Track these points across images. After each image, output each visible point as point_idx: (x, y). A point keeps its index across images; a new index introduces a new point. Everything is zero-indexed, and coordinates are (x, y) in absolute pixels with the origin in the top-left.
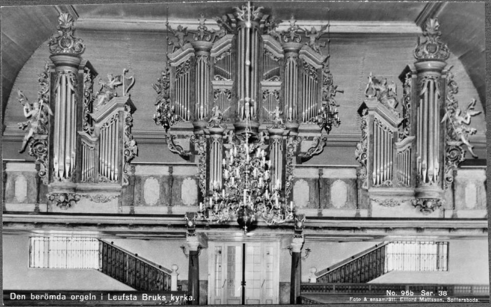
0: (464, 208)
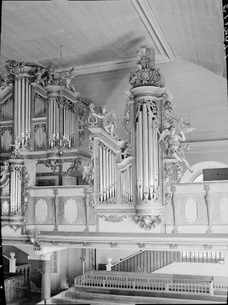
0: (186, 224)
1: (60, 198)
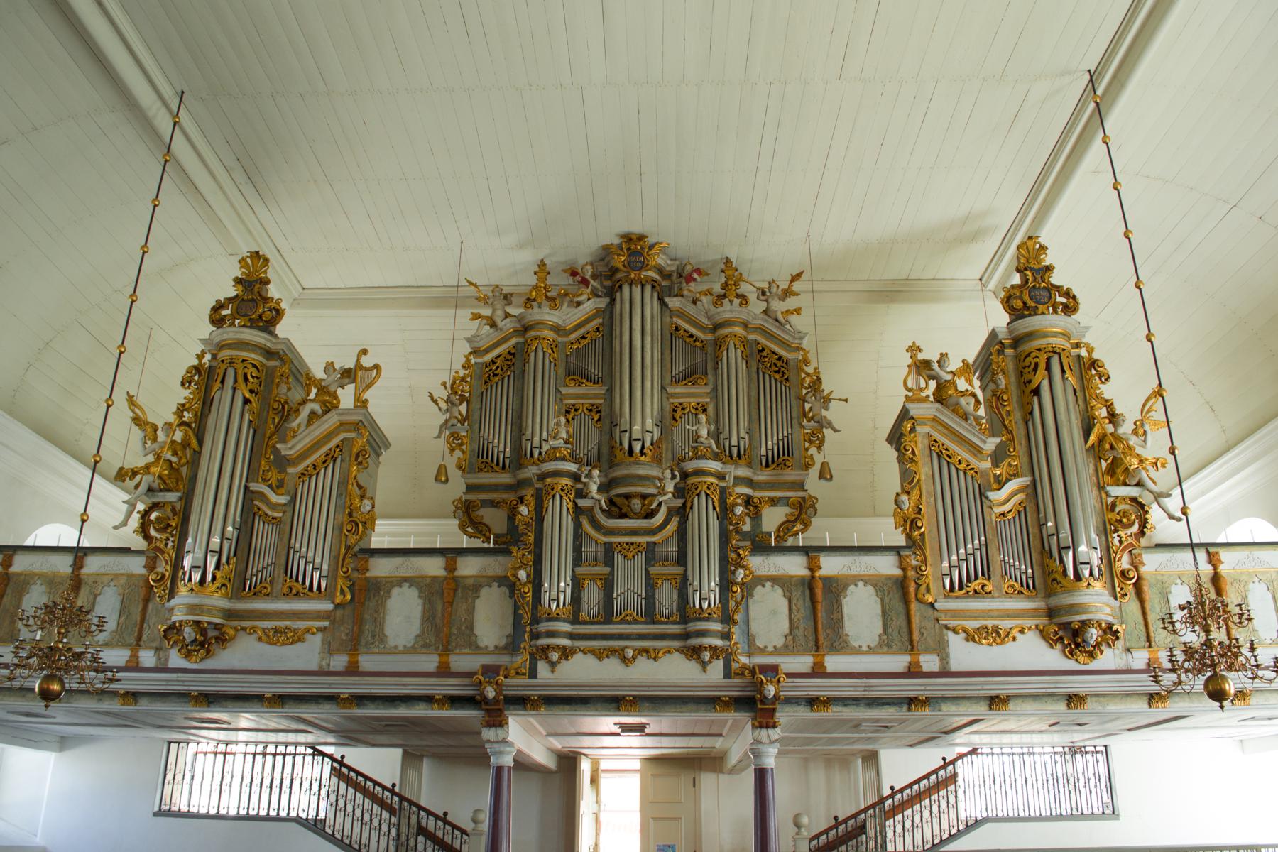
1: (828, 580)
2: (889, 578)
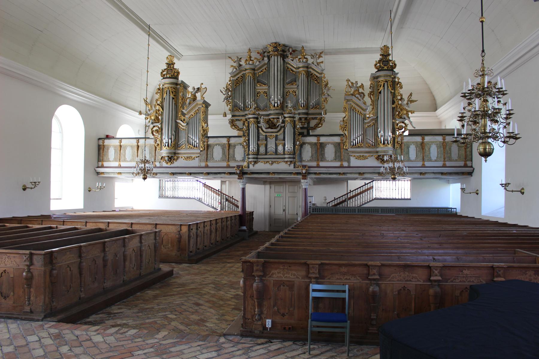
1: (321, 144)
2: (337, 143)
